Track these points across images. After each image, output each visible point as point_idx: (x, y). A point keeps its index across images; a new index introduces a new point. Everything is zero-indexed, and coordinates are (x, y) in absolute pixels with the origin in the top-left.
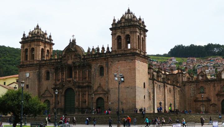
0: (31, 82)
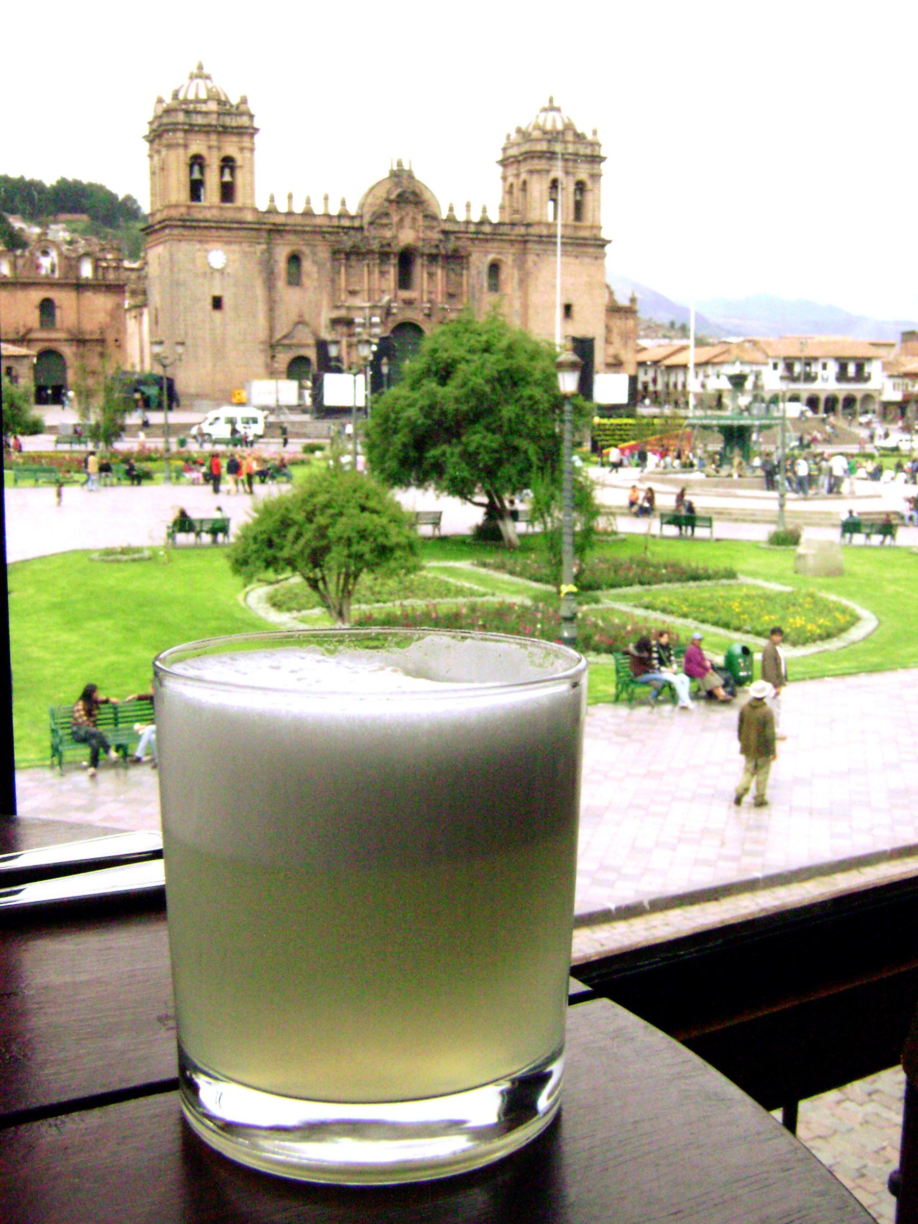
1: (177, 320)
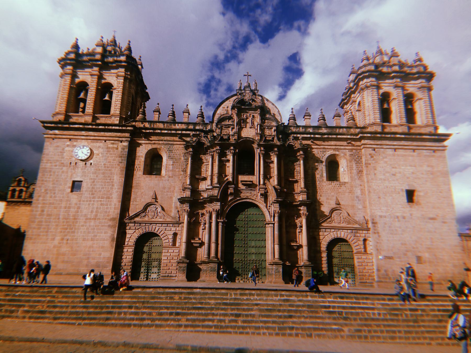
0: (95, 173)
1: (37, 200)
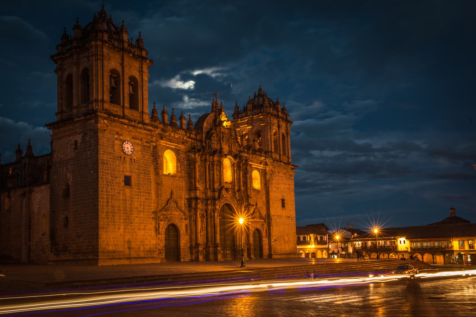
1: (102, 191)
